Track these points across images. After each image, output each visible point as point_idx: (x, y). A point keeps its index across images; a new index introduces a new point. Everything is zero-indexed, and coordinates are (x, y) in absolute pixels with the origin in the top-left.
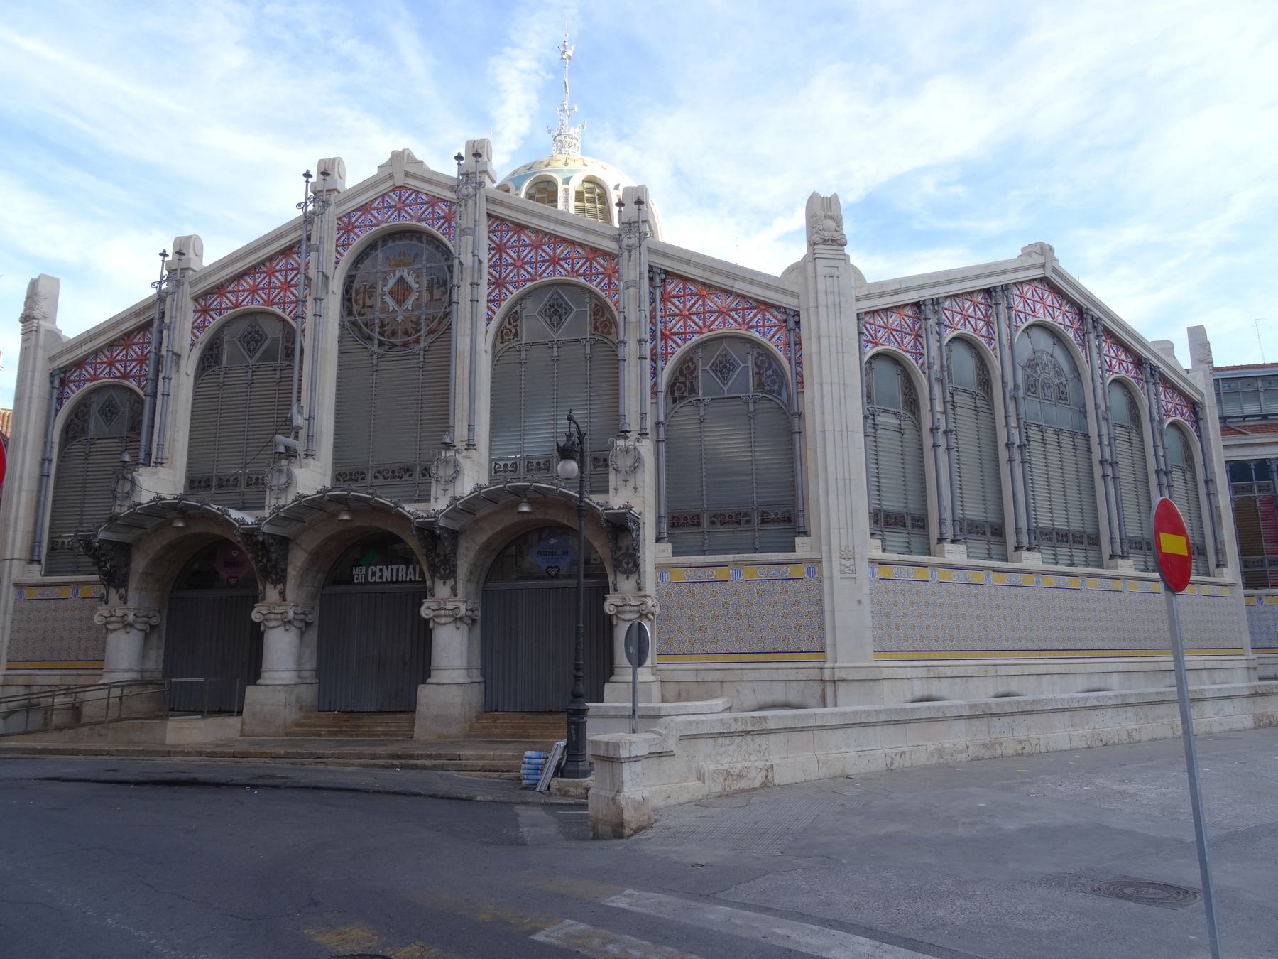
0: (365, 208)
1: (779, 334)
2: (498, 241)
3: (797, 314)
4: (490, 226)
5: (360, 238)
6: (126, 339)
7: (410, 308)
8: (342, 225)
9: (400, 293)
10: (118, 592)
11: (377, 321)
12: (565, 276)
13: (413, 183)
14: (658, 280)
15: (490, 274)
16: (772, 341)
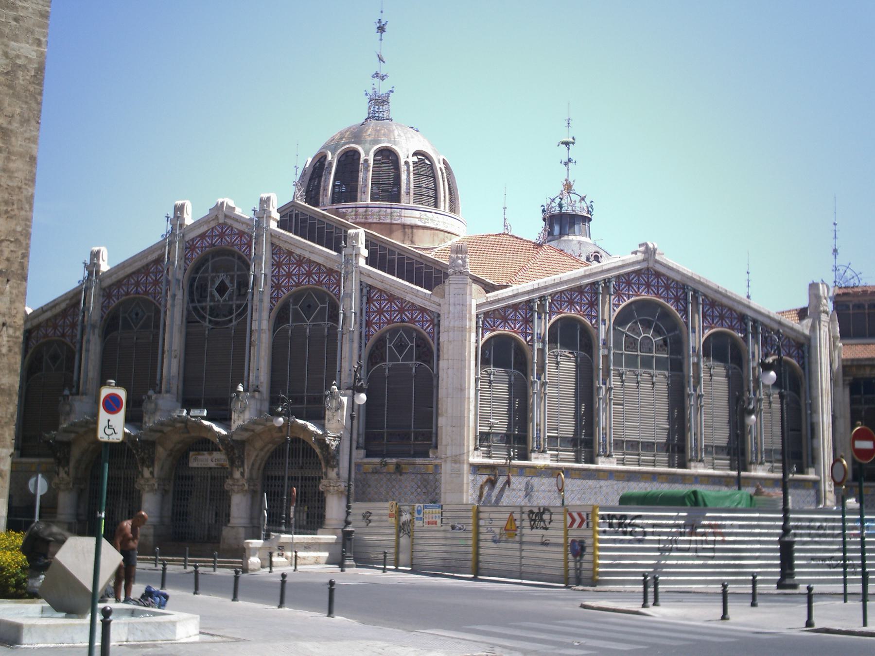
0: (202, 236)
1: (431, 326)
2: (277, 260)
3: (439, 315)
4: (273, 250)
5: (198, 254)
6: (64, 313)
7: (227, 299)
8: (189, 246)
9: (222, 289)
10: (64, 469)
11: (208, 307)
12: (315, 285)
13: (229, 222)
14: (365, 291)
15: (272, 280)
16: (426, 329)
